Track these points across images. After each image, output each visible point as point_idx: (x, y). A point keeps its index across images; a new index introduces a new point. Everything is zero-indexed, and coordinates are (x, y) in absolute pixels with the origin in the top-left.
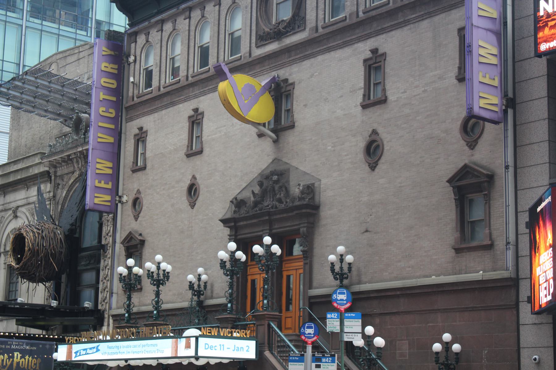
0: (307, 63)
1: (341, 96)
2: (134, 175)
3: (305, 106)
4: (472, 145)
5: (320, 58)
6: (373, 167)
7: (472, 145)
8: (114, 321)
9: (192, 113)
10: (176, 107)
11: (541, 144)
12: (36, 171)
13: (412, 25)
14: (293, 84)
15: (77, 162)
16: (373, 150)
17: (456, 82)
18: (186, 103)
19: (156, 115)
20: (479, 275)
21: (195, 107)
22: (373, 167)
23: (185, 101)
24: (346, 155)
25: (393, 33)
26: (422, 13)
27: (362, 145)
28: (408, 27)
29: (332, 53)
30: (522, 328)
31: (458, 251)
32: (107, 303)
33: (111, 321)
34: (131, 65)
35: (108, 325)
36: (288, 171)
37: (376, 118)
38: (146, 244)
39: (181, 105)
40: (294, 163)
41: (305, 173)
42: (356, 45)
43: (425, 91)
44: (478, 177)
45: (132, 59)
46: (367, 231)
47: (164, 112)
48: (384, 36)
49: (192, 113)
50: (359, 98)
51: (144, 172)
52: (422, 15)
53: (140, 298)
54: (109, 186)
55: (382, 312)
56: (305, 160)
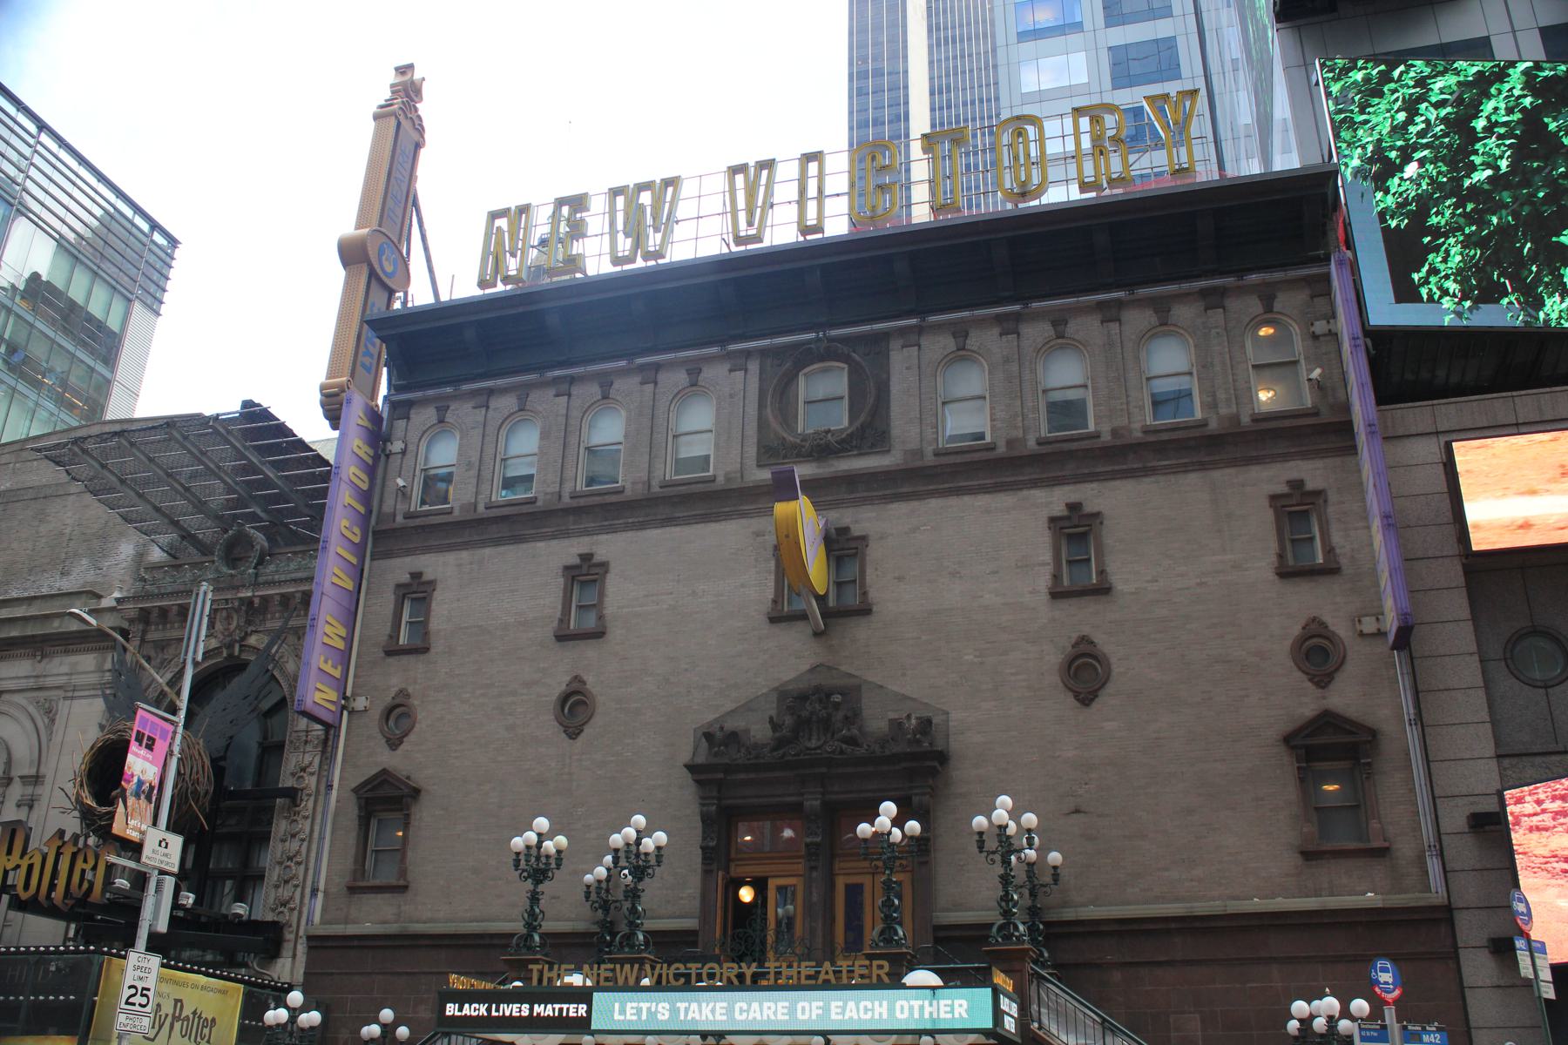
0: (899, 509)
2: (391, 660)
3: (900, 579)
4: (1323, 680)
5: (934, 503)
6: (1086, 699)
7: (1323, 680)
8: (310, 948)
9: (577, 561)
10: (524, 546)
11: (1471, 692)
12: (14, 633)
14: (863, 538)
15: (229, 617)
16: (1085, 673)
17: (1270, 575)
18: (554, 542)
19: (465, 555)
20: (1370, 898)
21: (586, 551)
22: (1086, 699)
23: (554, 537)
25: (1117, 483)
27: (1054, 658)
28: (1153, 479)
29: (966, 499)
30: (1468, 992)
31: (1309, 855)
32: (293, 910)
33: (301, 948)
34: (392, 458)
35: (294, 956)
36: (858, 688)
37: (1084, 618)
38: (424, 797)
39: (541, 545)
40: (874, 677)
41: (905, 698)
42: (1025, 493)
43: (1200, 584)
45: (397, 446)
47: (487, 551)
48: (1094, 485)
49: (577, 561)
50: (1043, 581)
51: (422, 657)
52: (1193, 463)
54: (337, 673)
55: (1129, 959)
56: (904, 675)
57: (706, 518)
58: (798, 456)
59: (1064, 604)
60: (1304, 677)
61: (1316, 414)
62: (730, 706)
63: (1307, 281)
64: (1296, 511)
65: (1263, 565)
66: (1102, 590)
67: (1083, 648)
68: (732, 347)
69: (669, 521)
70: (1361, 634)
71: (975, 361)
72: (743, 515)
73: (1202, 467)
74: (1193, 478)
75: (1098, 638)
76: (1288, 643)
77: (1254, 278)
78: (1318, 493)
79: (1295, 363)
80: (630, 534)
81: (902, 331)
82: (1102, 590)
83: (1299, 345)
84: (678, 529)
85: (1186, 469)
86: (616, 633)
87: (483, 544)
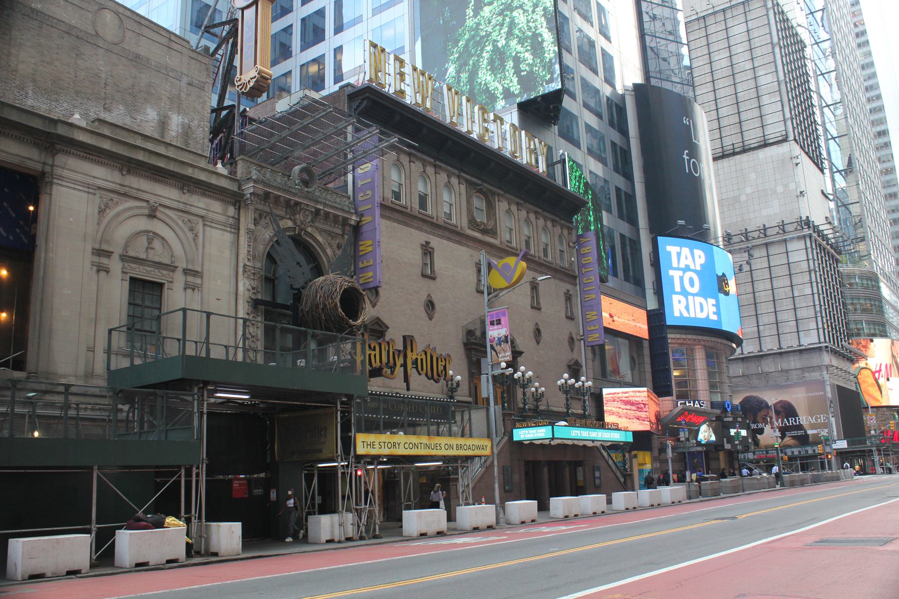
6: (538, 343)
16: (538, 332)
22: (538, 343)
57: (459, 243)
62: (470, 320)
64: (568, 298)
65: (563, 315)
66: (539, 309)
68: (462, 174)
69: (449, 239)
72: (468, 246)
77: (563, 222)
81: (499, 195)
82: (539, 309)
83: (565, 247)
87: (395, 220)
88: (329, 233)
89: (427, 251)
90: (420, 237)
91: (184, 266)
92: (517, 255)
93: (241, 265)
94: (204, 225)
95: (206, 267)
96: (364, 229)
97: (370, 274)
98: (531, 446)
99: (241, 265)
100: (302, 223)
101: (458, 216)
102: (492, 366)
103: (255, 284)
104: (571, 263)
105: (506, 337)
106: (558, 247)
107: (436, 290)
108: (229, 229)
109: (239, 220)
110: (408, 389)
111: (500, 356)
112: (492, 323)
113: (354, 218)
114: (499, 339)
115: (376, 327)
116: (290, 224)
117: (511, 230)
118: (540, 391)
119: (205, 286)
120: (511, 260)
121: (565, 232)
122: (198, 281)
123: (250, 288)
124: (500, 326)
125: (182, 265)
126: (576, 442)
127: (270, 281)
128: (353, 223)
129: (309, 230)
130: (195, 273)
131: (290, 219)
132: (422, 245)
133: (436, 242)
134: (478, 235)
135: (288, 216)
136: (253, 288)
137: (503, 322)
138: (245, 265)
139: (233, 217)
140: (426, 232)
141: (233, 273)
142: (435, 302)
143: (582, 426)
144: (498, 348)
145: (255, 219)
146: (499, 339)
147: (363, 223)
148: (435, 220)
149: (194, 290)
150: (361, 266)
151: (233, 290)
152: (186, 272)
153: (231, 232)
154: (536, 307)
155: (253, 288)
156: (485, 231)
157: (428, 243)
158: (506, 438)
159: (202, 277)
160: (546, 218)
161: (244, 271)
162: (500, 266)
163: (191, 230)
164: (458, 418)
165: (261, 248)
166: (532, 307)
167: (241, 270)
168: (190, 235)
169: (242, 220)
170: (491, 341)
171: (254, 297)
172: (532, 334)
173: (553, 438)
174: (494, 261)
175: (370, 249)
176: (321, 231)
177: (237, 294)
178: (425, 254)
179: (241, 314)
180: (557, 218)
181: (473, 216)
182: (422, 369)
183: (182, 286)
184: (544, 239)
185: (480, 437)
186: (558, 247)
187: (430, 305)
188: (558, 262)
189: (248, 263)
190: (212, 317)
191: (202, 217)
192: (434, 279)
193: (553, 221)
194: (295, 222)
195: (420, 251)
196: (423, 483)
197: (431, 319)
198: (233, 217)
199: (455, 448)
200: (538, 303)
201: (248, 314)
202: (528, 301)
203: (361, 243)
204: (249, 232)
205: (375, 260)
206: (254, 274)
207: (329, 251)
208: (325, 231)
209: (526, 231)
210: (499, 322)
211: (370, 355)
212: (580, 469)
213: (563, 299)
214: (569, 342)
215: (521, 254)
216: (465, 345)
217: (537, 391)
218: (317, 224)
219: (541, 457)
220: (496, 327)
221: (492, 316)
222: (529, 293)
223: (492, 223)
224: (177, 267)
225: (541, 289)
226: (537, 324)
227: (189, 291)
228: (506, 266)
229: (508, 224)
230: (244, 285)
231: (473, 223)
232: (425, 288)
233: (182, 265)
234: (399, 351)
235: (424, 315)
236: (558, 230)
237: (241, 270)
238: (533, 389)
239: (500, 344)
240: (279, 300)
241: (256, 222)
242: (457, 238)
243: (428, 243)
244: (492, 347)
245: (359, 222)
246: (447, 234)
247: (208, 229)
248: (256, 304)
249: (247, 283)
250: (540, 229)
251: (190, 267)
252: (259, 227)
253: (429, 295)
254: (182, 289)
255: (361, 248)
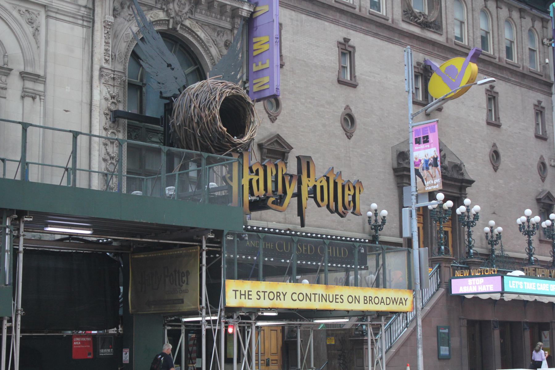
1: (473, 107)
4: (543, 179)
6: (496, 169)
7: (543, 179)
10: (320, 21)
13: (511, 84)
18: (332, 25)
21: (346, 37)
22: (496, 169)
24: (479, 153)
25: (501, 82)
26: (517, 81)
27: (487, 150)
39: (327, 24)
44: (551, 201)
46: (494, 213)
47: (304, 16)
49: (342, 41)
53: (285, 215)
57: (389, 40)
58: (416, 22)
59: (491, 128)
60: (540, 177)
61: (542, 76)
63: (543, 20)
64: (539, 111)
66: (498, 126)
67: (494, 149)
69: (376, 35)
70: (551, 165)
71: (461, 3)
73: (521, 85)
74: (518, 88)
75: (498, 145)
76: (537, 163)
77: (534, 12)
78: (543, 108)
79: (534, 51)
80: (362, 35)
83: (537, 45)
84: (379, 40)
85: (516, 84)
86: (360, 88)
88: (214, 28)
89: (346, 50)
90: (338, 32)
91: (22, 68)
92: (466, 55)
93: (96, 67)
94: (48, 16)
95: (50, 70)
96: (260, 22)
97: (266, 79)
98: (476, 301)
99: (96, 67)
100: (177, 14)
101: (389, 6)
102: (417, 196)
103: (115, 91)
104: (545, 66)
105: (435, 159)
106: (527, 45)
107: (358, 102)
108: (80, 22)
109: (94, 10)
110: (303, 225)
111: (427, 183)
112: (418, 141)
113: (246, 7)
114: (427, 161)
115: (277, 147)
116: (162, 15)
117: (462, 23)
118: (496, 231)
119: (49, 93)
120: (458, 62)
121: (538, 25)
122: (40, 87)
123: (108, 96)
124: (427, 145)
125: (18, 66)
126: (538, 299)
127: (135, 88)
128: (244, 14)
129: (187, 23)
130: (36, 78)
131: (162, 9)
132: (339, 43)
133: (358, 39)
134: (416, 30)
135: (159, 6)
136: (113, 97)
137: (431, 139)
138: (101, 68)
139: (85, 7)
140: (345, 26)
141: (86, 78)
142: (356, 116)
143: (544, 278)
144: (424, 173)
145: (114, 10)
146: (427, 161)
147: (258, 14)
148: (357, 11)
149: (34, 98)
150: (255, 69)
151: (86, 99)
152: (24, 76)
153: (83, 26)
154: (494, 123)
155: (113, 97)
156: (425, 25)
157: (346, 40)
158: (442, 290)
159: (44, 83)
160: (510, 8)
161: (101, 76)
162: (443, 70)
163: (31, 22)
164: (371, 262)
165: (123, 46)
166: (489, 123)
167: (96, 74)
168: (29, 30)
169: (98, 10)
170: (417, 164)
171: (113, 108)
172: (487, 158)
173: (502, 293)
174: (436, 63)
175: (266, 47)
176: (203, 25)
177: (91, 105)
178: (343, 54)
179: (96, 130)
180: (527, 8)
181: (409, 6)
182: (322, 199)
183: (19, 93)
184: (507, 34)
185: (398, 287)
186: (527, 45)
187: (349, 120)
188: (527, 64)
189: (105, 66)
190: (29, 129)
191: (44, 6)
192: (355, 86)
193: (521, 10)
194: (167, 12)
195: (335, 51)
196: (330, 345)
197: (349, 137)
198: (85, 7)
199: (362, 300)
200: (497, 118)
201: (105, 129)
202: (483, 116)
203: (255, 40)
204: (107, 25)
205: (272, 63)
206: (114, 79)
207: (214, 51)
208: (209, 25)
209: (482, 24)
210: (426, 140)
211: (251, 181)
212: (546, 333)
213: (531, 113)
214: (540, 169)
215: (471, 53)
216: (395, 170)
217: (492, 231)
218: (198, 16)
219: (490, 316)
220: (422, 146)
221: (417, 132)
222: (485, 106)
223: (435, 14)
224: (11, 70)
225: (502, 100)
226: (494, 145)
227: (28, 100)
228: (451, 69)
229: (458, 15)
230: (101, 93)
231: (409, 15)
232: (342, 97)
233: (18, 66)
234: (291, 176)
235: (340, 132)
236: (527, 22)
237: (96, 74)
238: (487, 229)
239: (427, 169)
240: (149, 113)
241: (116, 13)
242: (386, 33)
243: (346, 40)
244: (417, 173)
245: (253, 13)
246: (373, 28)
247: (51, 21)
248: (115, 116)
249: (105, 90)
250: (502, 22)
251: (29, 70)
252: (120, 20)
253: (347, 107)
254: (18, 97)
255: (255, 47)
